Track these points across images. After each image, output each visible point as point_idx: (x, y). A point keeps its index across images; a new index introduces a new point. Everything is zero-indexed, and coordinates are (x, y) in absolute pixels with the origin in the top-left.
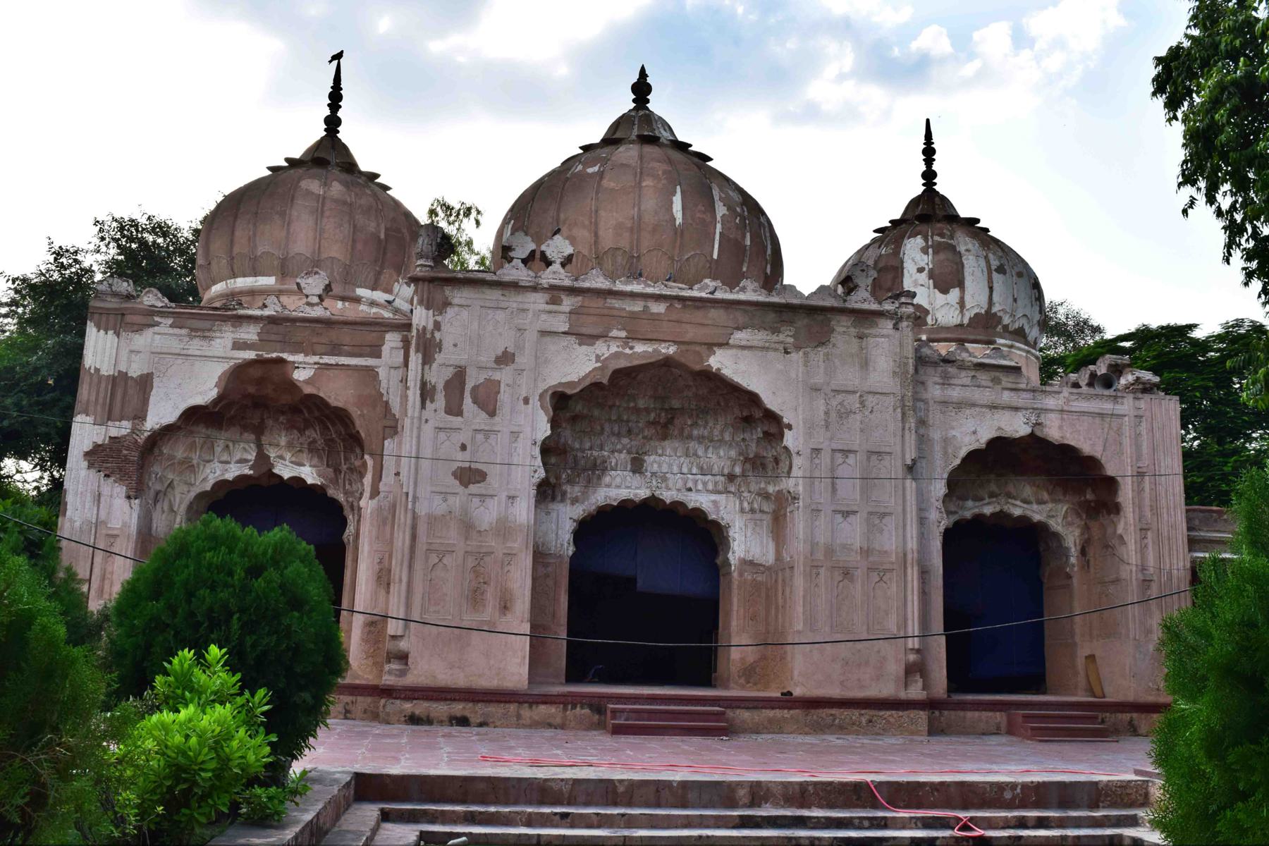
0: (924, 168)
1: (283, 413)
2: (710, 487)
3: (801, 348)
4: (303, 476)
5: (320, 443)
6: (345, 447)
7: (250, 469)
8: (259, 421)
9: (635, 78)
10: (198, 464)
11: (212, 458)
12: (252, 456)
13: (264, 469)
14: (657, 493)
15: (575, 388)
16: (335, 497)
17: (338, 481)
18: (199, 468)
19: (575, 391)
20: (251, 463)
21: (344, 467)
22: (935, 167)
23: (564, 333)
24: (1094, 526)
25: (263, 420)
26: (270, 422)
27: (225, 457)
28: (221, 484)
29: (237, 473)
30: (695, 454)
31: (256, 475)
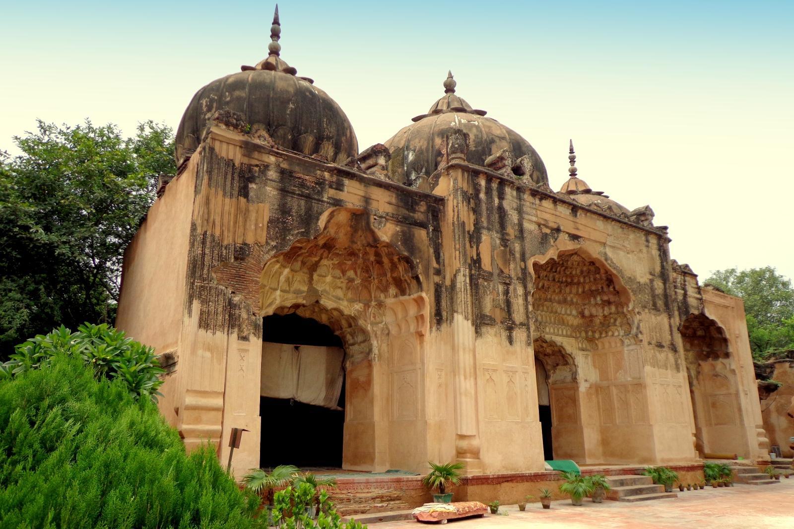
0: (569, 166)
1: (338, 255)
2: (564, 333)
3: (633, 252)
4: (342, 308)
5: (358, 281)
6: (378, 288)
7: (304, 299)
8: (316, 259)
9: (445, 78)
10: (268, 291)
11: (276, 287)
12: (305, 288)
13: (314, 300)
14: (543, 335)
15: (543, 261)
16: (364, 326)
17: (366, 314)
18: (267, 294)
19: (544, 262)
20: (304, 294)
21: (373, 303)
22: (576, 165)
23: (535, 222)
24: (706, 366)
25: (321, 258)
26: (325, 262)
27: (284, 288)
28: (282, 308)
29: (294, 301)
30: (556, 312)
31: (308, 305)
